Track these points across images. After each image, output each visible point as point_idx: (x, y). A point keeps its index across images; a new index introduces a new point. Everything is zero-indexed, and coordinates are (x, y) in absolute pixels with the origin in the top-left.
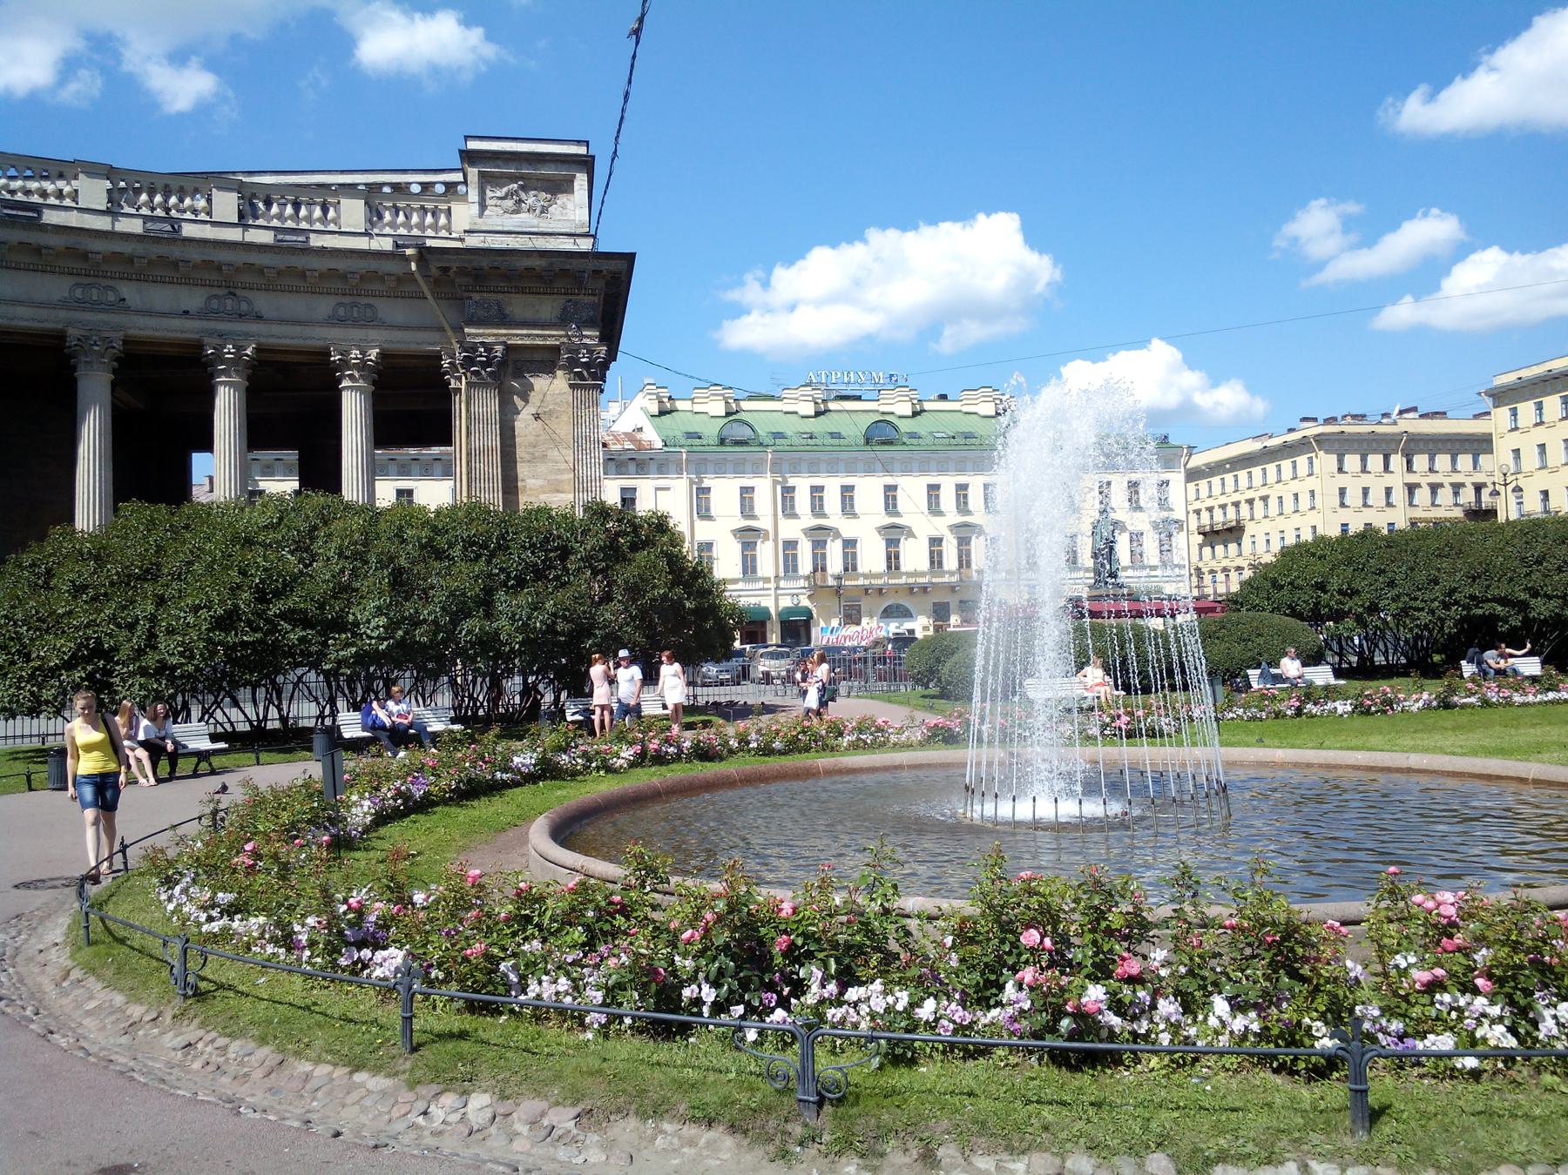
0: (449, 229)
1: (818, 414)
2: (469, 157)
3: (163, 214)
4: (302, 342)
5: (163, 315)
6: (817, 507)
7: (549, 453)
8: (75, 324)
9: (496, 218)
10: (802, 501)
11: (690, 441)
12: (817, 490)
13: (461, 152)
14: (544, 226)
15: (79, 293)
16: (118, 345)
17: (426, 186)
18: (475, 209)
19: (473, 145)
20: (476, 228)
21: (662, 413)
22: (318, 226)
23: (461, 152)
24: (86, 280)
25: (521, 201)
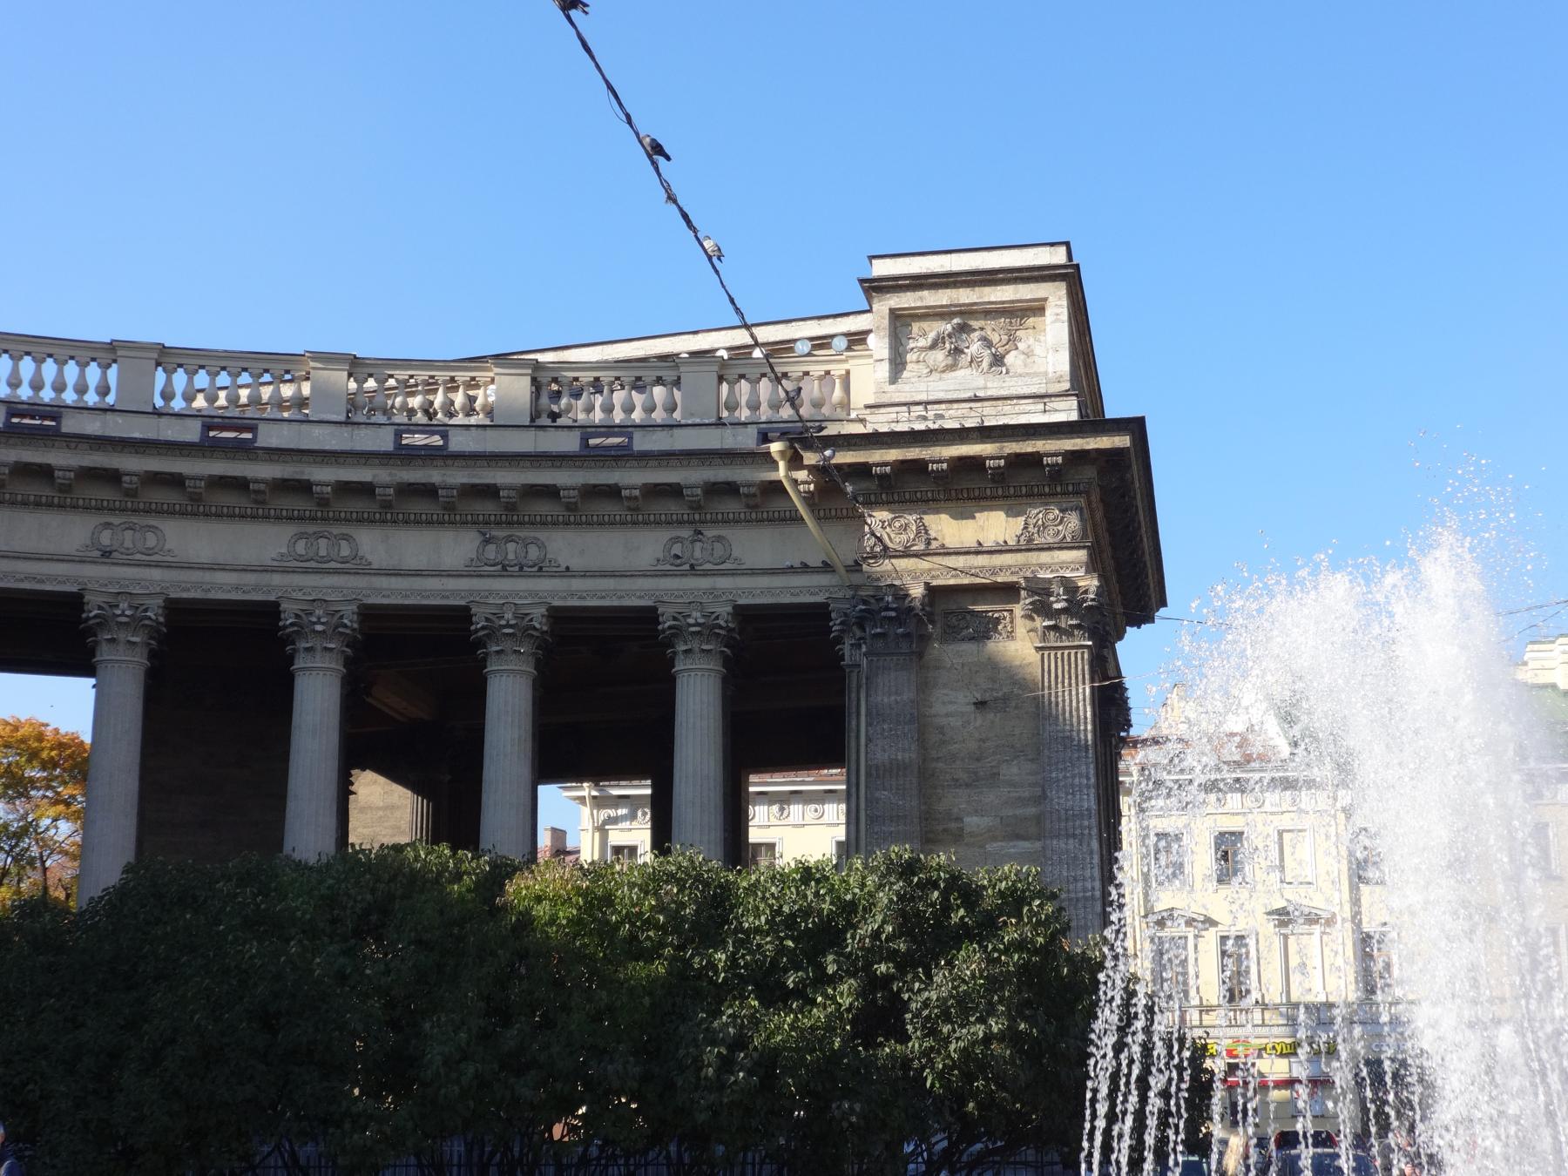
2: (875, 287)
3: (425, 420)
4: (616, 603)
5: (418, 573)
7: (1004, 769)
8: (294, 591)
9: (920, 382)
13: (862, 281)
15: (301, 547)
16: (350, 620)
18: (884, 370)
19: (882, 268)
20: (885, 399)
23: (862, 281)
24: (311, 528)
25: (957, 351)
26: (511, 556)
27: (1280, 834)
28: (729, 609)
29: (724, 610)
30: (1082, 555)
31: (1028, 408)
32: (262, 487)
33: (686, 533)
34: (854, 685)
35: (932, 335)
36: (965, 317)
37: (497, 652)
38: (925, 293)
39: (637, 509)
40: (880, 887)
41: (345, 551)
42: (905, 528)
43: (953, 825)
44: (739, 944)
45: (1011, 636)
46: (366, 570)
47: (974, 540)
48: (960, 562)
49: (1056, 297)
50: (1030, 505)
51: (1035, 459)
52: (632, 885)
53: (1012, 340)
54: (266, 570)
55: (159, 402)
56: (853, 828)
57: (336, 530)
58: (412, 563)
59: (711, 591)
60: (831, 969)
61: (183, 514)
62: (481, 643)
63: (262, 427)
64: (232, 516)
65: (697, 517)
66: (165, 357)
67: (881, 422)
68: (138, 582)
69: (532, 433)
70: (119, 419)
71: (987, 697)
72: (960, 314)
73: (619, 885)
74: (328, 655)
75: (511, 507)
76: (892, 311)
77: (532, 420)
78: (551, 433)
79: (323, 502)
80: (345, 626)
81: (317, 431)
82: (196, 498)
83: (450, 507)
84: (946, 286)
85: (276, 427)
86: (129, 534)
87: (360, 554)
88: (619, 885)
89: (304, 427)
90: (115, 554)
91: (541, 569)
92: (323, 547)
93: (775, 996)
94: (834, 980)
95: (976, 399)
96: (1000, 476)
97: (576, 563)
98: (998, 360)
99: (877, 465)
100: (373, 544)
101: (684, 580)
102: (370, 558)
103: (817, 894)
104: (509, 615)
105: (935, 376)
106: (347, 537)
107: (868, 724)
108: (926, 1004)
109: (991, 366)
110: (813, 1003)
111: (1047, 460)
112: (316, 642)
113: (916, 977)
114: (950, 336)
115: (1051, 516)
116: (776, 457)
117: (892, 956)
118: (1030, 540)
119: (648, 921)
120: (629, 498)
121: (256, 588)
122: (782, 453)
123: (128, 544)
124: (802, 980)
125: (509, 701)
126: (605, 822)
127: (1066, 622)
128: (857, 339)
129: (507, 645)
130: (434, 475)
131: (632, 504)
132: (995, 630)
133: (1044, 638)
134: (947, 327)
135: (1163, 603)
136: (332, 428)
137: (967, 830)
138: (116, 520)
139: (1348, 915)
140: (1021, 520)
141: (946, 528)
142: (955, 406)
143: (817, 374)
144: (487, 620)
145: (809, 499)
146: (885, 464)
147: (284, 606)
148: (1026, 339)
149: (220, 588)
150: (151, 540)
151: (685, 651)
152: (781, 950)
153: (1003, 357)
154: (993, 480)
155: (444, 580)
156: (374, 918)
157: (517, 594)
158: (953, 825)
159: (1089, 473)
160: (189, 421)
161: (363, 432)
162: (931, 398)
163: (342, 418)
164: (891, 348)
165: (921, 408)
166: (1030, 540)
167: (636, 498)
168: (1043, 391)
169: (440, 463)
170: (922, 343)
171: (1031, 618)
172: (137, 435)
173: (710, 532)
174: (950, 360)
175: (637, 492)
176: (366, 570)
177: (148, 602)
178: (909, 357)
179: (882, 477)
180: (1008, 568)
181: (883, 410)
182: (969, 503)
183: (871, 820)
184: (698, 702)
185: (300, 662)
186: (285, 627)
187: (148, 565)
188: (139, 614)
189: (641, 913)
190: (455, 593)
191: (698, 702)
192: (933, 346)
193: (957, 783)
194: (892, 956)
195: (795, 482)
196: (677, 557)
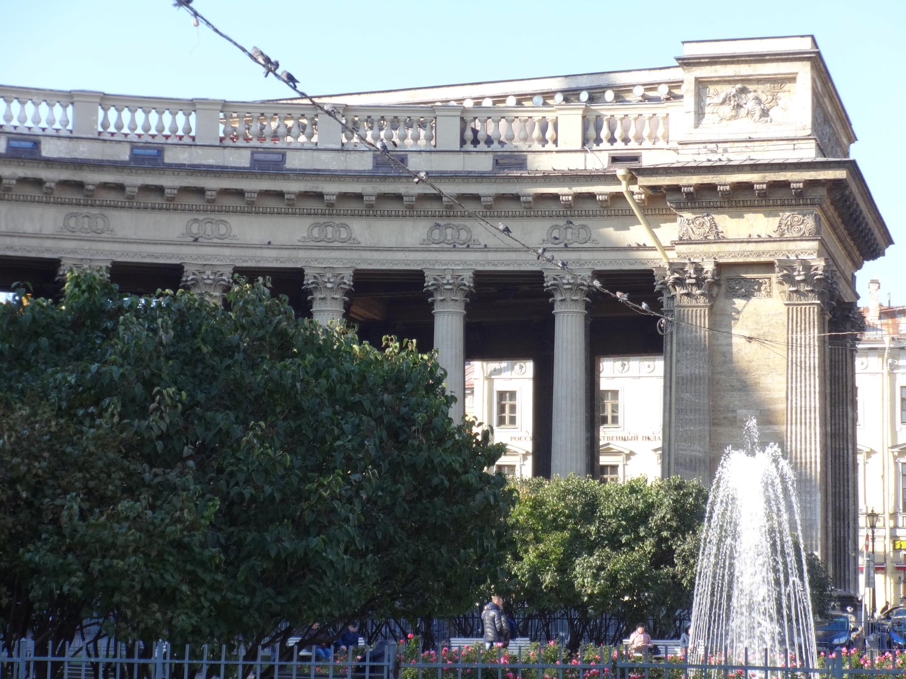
2: (686, 63)
4: (516, 268)
5: (390, 249)
9: (712, 128)
14: (762, 130)
17: (651, 86)
22: (537, 146)
24: (322, 220)
25: (739, 106)
30: (815, 245)
32: (293, 196)
33: (562, 222)
35: (722, 96)
36: (744, 84)
37: (442, 300)
38: (718, 67)
39: (530, 208)
40: (665, 496)
42: (703, 224)
43: (730, 415)
44: (601, 523)
45: (769, 294)
47: (748, 232)
48: (738, 247)
49: (804, 71)
50: (783, 211)
52: (553, 496)
53: (774, 98)
56: (667, 414)
57: (338, 221)
58: (387, 242)
60: (642, 534)
62: (431, 294)
63: (289, 155)
65: (569, 213)
68: (215, 257)
70: (200, 151)
73: (548, 496)
74: (334, 301)
76: (697, 79)
77: (461, 146)
79: (331, 205)
80: (345, 283)
81: (324, 156)
84: (732, 63)
85: (298, 153)
86: (209, 225)
87: (353, 236)
88: (548, 496)
89: (316, 153)
90: (200, 240)
91: (468, 246)
93: (616, 545)
94: (642, 539)
95: (750, 140)
96: (763, 195)
98: (765, 113)
99: (685, 186)
100: (363, 230)
102: (359, 239)
103: (637, 499)
104: (449, 277)
106: (344, 226)
107: (678, 351)
108: (683, 551)
109: (761, 117)
110: (633, 549)
112: (329, 295)
113: (679, 539)
114: (734, 96)
115: (796, 219)
116: (620, 178)
117: (670, 528)
118: (782, 235)
119: (560, 513)
120: (525, 202)
121: (289, 259)
122: (624, 177)
123: (209, 232)
124: (629, 539)
126: (491, 374)
127: (804, 288)
131: (527, 206)
132: (759, 290)
133: (790, 298)
134: (731, 89)
135: (890, 242)
137: (739, 417)
140: (778, 219)
141: (728, 225)
142: (737, 144)
143: (647, 116)
145: (641, 205)
146: (690, 186)
147: (306, 272)
149: (266, 260)
150: (223, 230)
151: (562, 300)
152: (620, 526)
153: (768, 110)
154: (759, 196)
155: (407, 253)
157: (453, 262)
158: (730, 415)
159: (822, 192)
160: (243, 151)
161: (353, 156)
162: (722, 138)
163: (339, 147)
165: (714, 145)
166: (782, 235)
167: (530, 202)
168: (792, 135)
169: (404, 180)
171: (781, 283)
172: (211, 162)
173: (577, 222)
174: (734, 113)
175: (530, 199)
177: (223, 270)
178: (708, 110)
179: (688, 194)
183: (679, 411)
184: (569, 330)
188: (217, 278)
190: (414, 262)
191: (569, 330)
192: (723, 103)
194: (670, 528)
195: (632, 193)
196: (556, 238)
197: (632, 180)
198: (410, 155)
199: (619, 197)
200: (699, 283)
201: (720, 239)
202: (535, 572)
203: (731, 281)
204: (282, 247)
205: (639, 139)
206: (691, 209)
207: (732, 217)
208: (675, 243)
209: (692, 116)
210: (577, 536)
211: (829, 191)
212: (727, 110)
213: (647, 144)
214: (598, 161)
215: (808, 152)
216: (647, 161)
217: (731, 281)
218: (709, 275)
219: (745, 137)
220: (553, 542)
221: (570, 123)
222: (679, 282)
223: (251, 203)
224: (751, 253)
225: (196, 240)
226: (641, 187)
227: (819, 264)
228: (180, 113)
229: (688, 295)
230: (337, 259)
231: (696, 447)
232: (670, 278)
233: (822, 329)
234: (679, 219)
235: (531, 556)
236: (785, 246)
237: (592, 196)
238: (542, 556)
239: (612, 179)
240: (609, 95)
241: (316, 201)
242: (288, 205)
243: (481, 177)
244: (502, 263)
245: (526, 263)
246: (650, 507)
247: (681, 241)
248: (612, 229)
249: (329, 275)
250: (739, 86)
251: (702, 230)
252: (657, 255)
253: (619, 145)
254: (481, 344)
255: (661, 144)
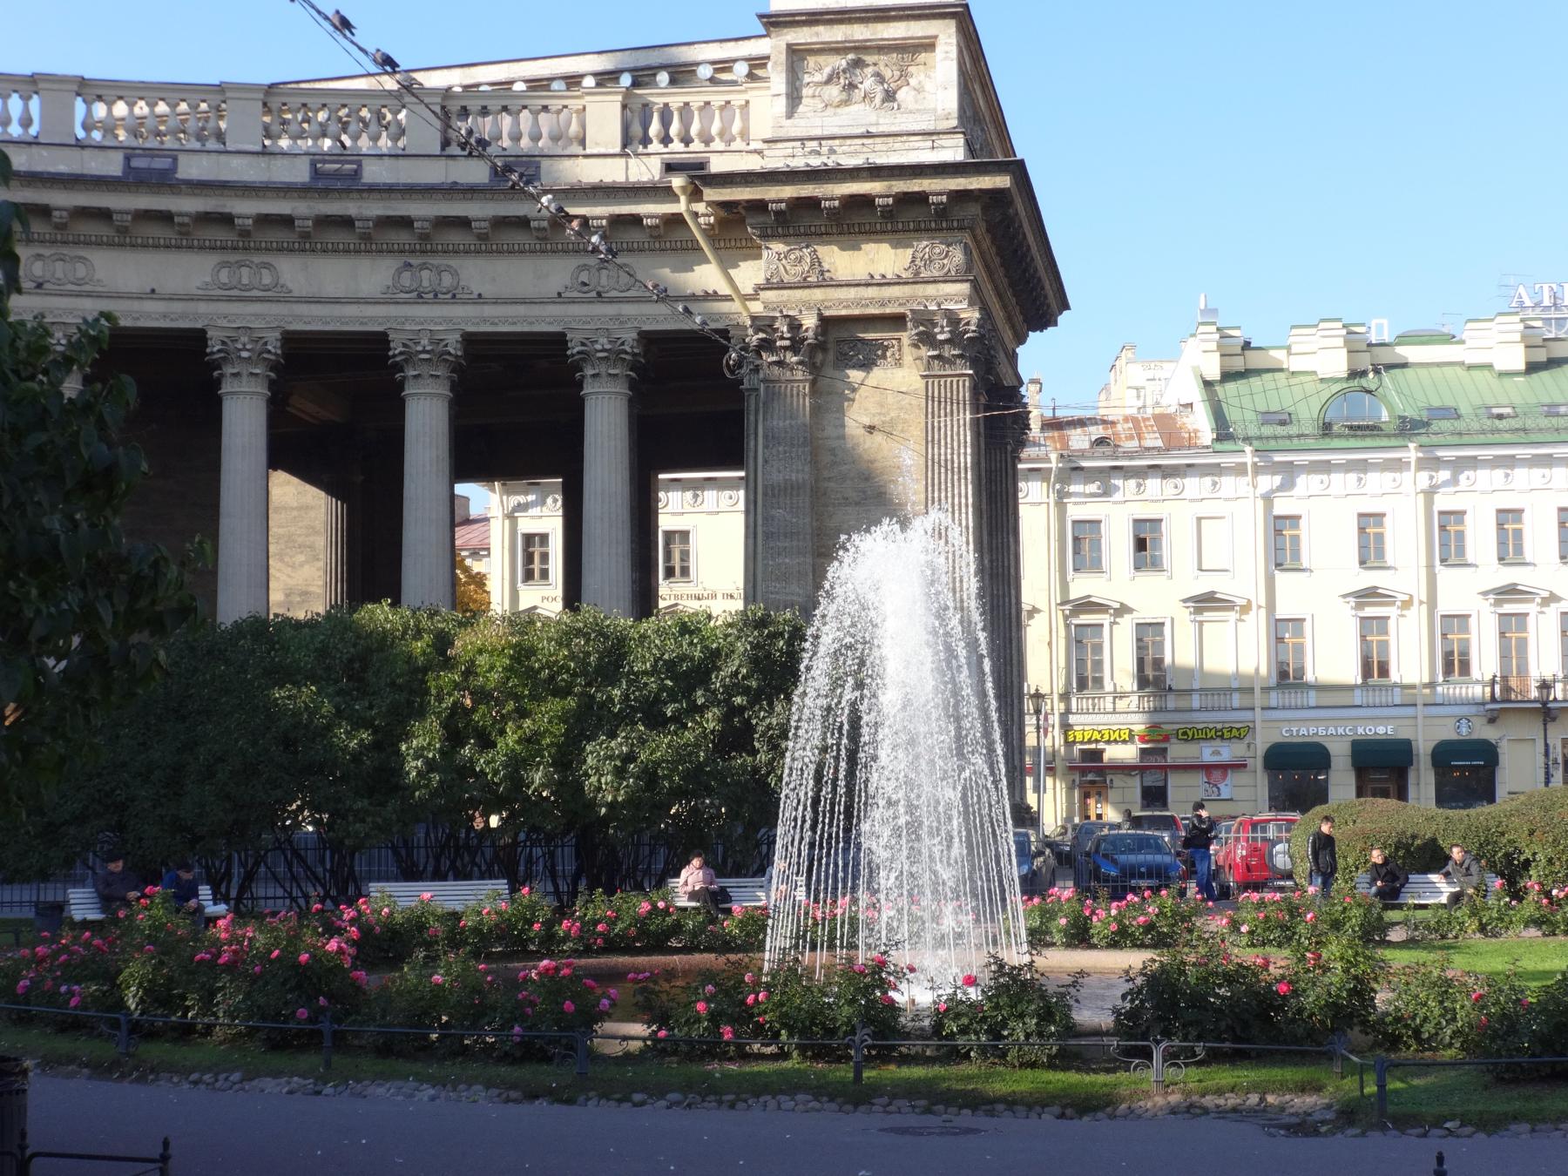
0: (745, 135)
1: (1532, 368)
2: (774, 22)
4: (526, 329)
5: (336, 301)
6: (1510, 547)
8: (221, 319)
9: (815, 118)
10: (1481, 538)
11: (1267, 431)
12: (1508, 518)
13: (761, 16)
14: (887, 122)
15: (224, 276)
16: (274, 347)
17: (724, 65)
18: (781, 104)
20: (782, 134)
21: (1227, 376)
23: (761, 16)
25: (852, 86)
26: (425, 283)
27: (1199, 519)
28: (634, 335)
29: (630, 336)
30: (965, 288)
31: (917, 145)
32: (186, 220)
34: (753, 407)
35: (827, 71)
37: (415, 377)
38: (821, 29)
39: (545, 239)
40: (739, 638)
41: (267, 279)
42: (800, 260)
45: (898, 363)
46: (288, 299)
47: (868, 269)
48: (852, 293)
49: (946, 36)
51: (921, 198)
52: (550, 640)
53: (904, 75)
54: (191, 298)
55: (81, 134)
56: (751, 541)
57: (257, 259)
58: (330, 290)
59: (617, 318)
60: (700, 701)
61: (111, 245)
62: (399, 367)
64: (156, 246)
66: (86, 88)
67: (776, 160)
69: (442, 162)
70: (44, 152)
71: (876, 421)
72: (855, 49)
73: (540, 639)
74: (253, 379)
75: (425, 237)
76: (789, 46)
77: (443, 149)
78: (462, 163)
79: (245, 233)
81: (236, 161)
82: (123, 231)
83: (366, 237)
84: (841, 22)
85: (196, 157)
86: (59, 265)
87: (281, 281)
88: (540, 639)
89: (223, 158)
90: (46, 286)
92: (245, 275)
93: (656, 721)
94: (701, 710)
95: (869, 135)
96: (889, 214)
97: (488, 291)
98: (890, 96)
99: (773, 202)
100: (294, 272)
101: (591, 306)
102: (290, 285)
103: (691, 643)
104: (425, 342)
105: (830, 110)
106: (267, 266)
107: (766, 447)
108: (769, 727)
109: (883, 102)
110: (685, 726)
111: (933, 199)
112: (245, 369)
113: (761, 708)
114: (844, 71)
116: (678, 191)
117: (746, 691)
118: (917, 274)
119: (562, 667)
120: (538, 229)
121: (184, 316)
122: (683, 188)
123: (59, 274)
124: (678, 710)
125: (426, 420)
126: (515, 509)
127: (950, 351)
128: (757, 64)
129: (425, 370)
130: (350, 208)
131: (540, 235)
132: (884, 357)
133: (929, 368)
134: (841, 62)
135: (1065, 305)
136: (249, 158)
138: (46, 252)
139: (1263, 602)
140: (910, 251)
141: (841, 261)
142: (848, 142)
143: (718, 104)
144: (405, 345)
145: (709, 232)
146: (780, 201)
147: (210, 334)
148: (917, 75)
149: (149, 316)
150: (81, 271)
151: (593, 376)
152: (663, 688)
154: (883, 216)
155: (363, 307)
156: (357, 665)
157: (432, 320)
159: (974, 210)
160: (111, 154)
161: (279, 162)
162: (826, 133)
163: (258, 148)
164: (788, 83)
165: (815, 143)
166: (917, 274)
168: (930, 127)
169: (355, 195)
170: (818, 77)
171: (916, 346)
172: (62, 168)
174: (844, 96)
176: (288, 299)
178: (805, 92)
179: (778, 213)
180: (895, 299)
181: (779, 145)
182: (860, 237)
183: (768, 536)
184: (606, 422)
185: (227, 387)
186: (212, 353)
187: (79, 295)
189: (557, 661)
191: (606, 422)
192: (828, 81)
193: (846, 501)
194: (746, 691)
195: (696, 215)
196: (585, 284)
197: (696, 195)
198: (365, 161)
199: (676, 221)
200: (795, 346)
201: (825, 282)
202: (517, 764)
203: (844, 343)
204: (171, 298)
205: (707, 141)
206: (782, 237)
207: (843, 249)
208: (759, 288)
209: (783, 101)
210: (587, 702)
211: (985, 209)
212: (834, 92)
213: (717, 145)
214: (645, 169)
215: (953, 151)
216: (718, 165)
217: (844, 343)
218: (810, 334)
219: (861, 130)
220: (547, 716)
221: (603, 117)
222: (767, 345)
223: (123, 231)
224: (872, 301)
225: (39, 286)
226: (709, 204)
227: (972, 315)
228: (15, 97)
229: (780, 363)
230: (257, 315)
231: (794, 588)
232: (754, 339)
233: (976, 408)
234: (765, 253)
235: (510, 740)
236: (921, 290)
237: (636, 220)
238: (530, 740)
239: (666, 193)
240: (663, 78)
241: (218, 228)
242: (180, 233)
243: (470, 191)
244: (505, 320)
245: (542, 320)
246: (714, 657)
247: (769, 286)
248: (667, 271)
249: (244, 339)
250: (851, 56)
251: (799, 269)
252: (735, 306)
253: (677, 146)
254: (483, 453)
255: (738, 144)
